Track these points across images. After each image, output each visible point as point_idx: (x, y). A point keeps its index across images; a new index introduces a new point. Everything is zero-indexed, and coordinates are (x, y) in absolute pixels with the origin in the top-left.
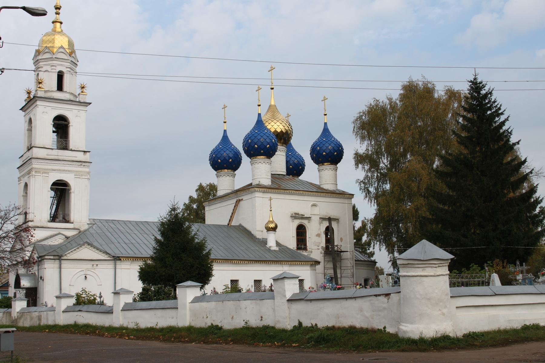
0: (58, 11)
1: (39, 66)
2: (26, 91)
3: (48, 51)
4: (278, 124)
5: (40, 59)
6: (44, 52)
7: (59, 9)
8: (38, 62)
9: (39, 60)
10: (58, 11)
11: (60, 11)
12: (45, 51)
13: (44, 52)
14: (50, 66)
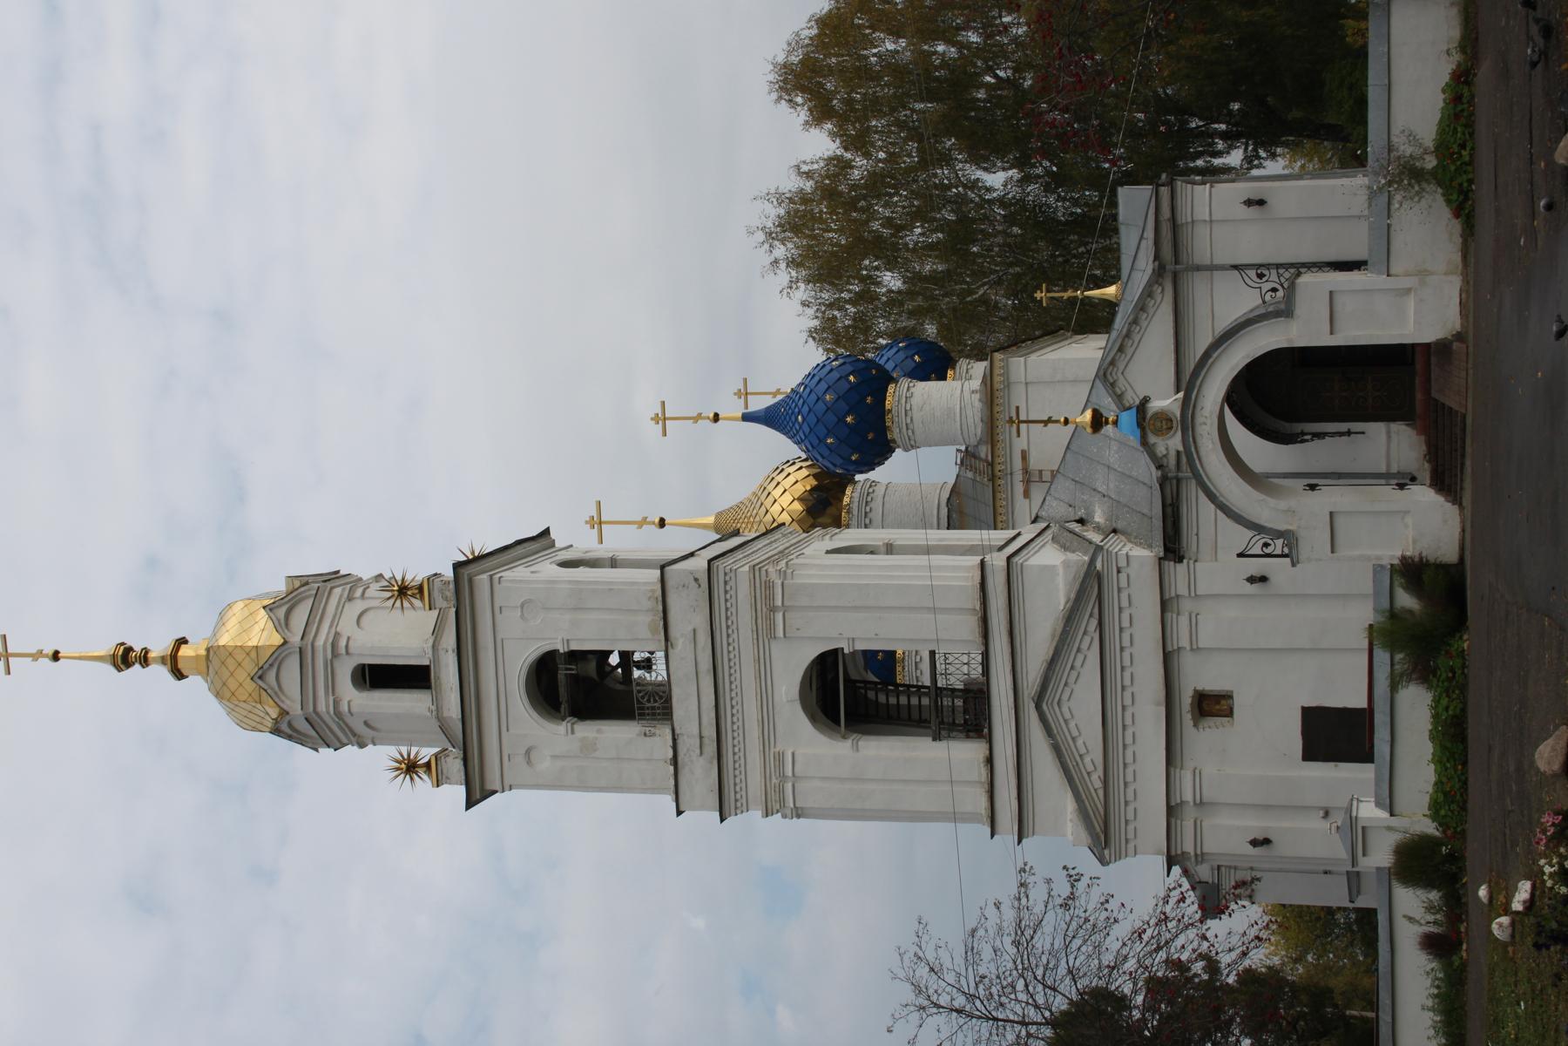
0: (134, 654)
1: (330, 640)
2: (398, 769)
3: (284, 609)
4: (777, 493)
5: (302, 638)
6: (281, 627)
7: (129, 650)
8: (309, 647)
9: (304, 642)
10: (134, 654)
11: (138, 648)
12: (279, 621)
13: (280, 624)
14: (347, 605)
